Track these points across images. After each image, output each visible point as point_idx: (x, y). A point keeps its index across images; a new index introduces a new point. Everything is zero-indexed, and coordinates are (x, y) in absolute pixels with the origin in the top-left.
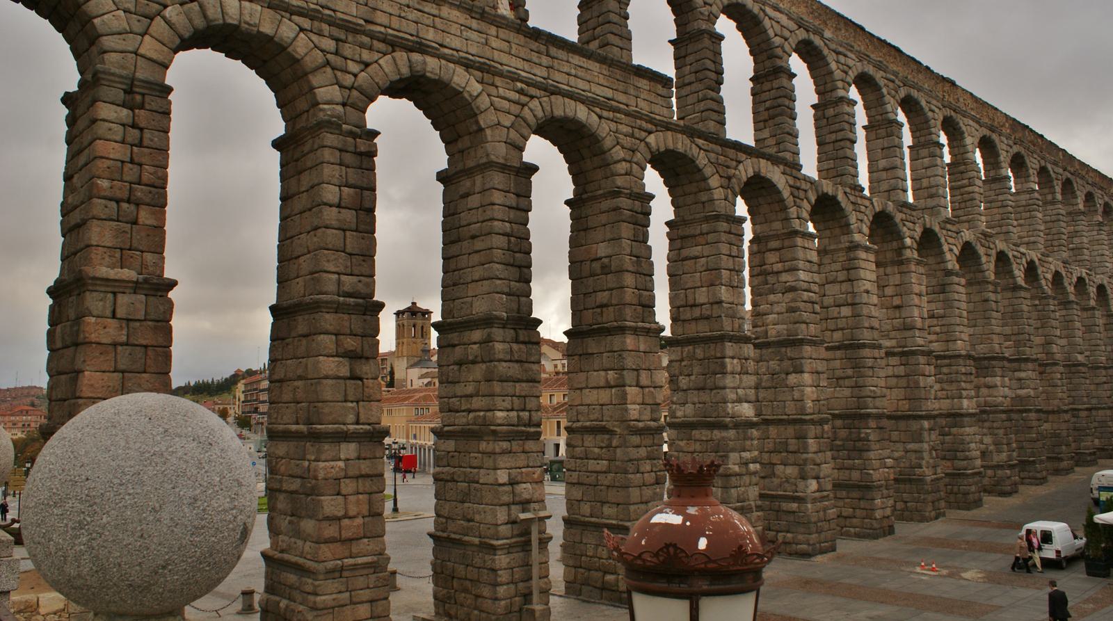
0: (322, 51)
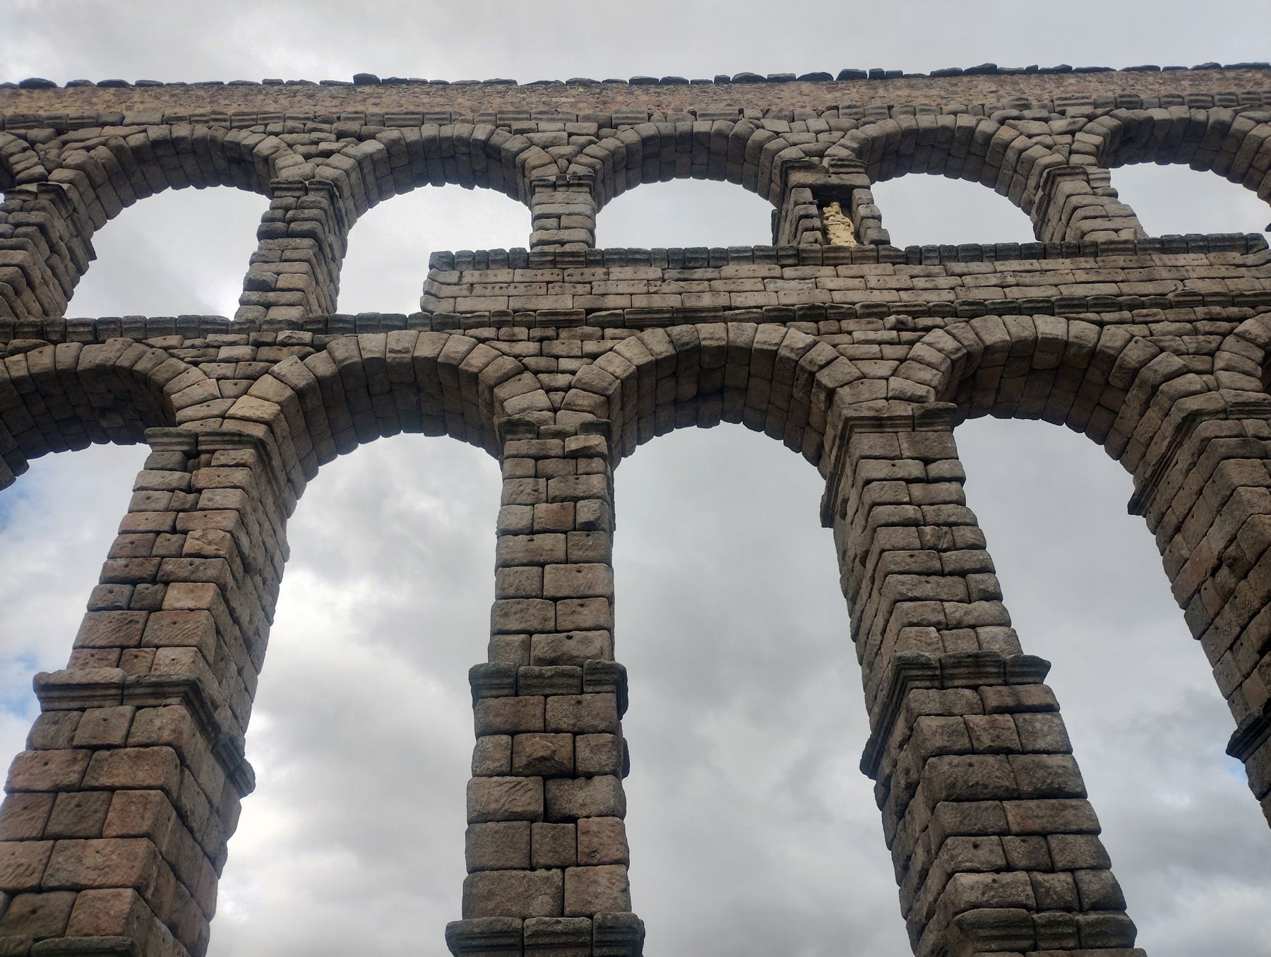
0: (516, 357)
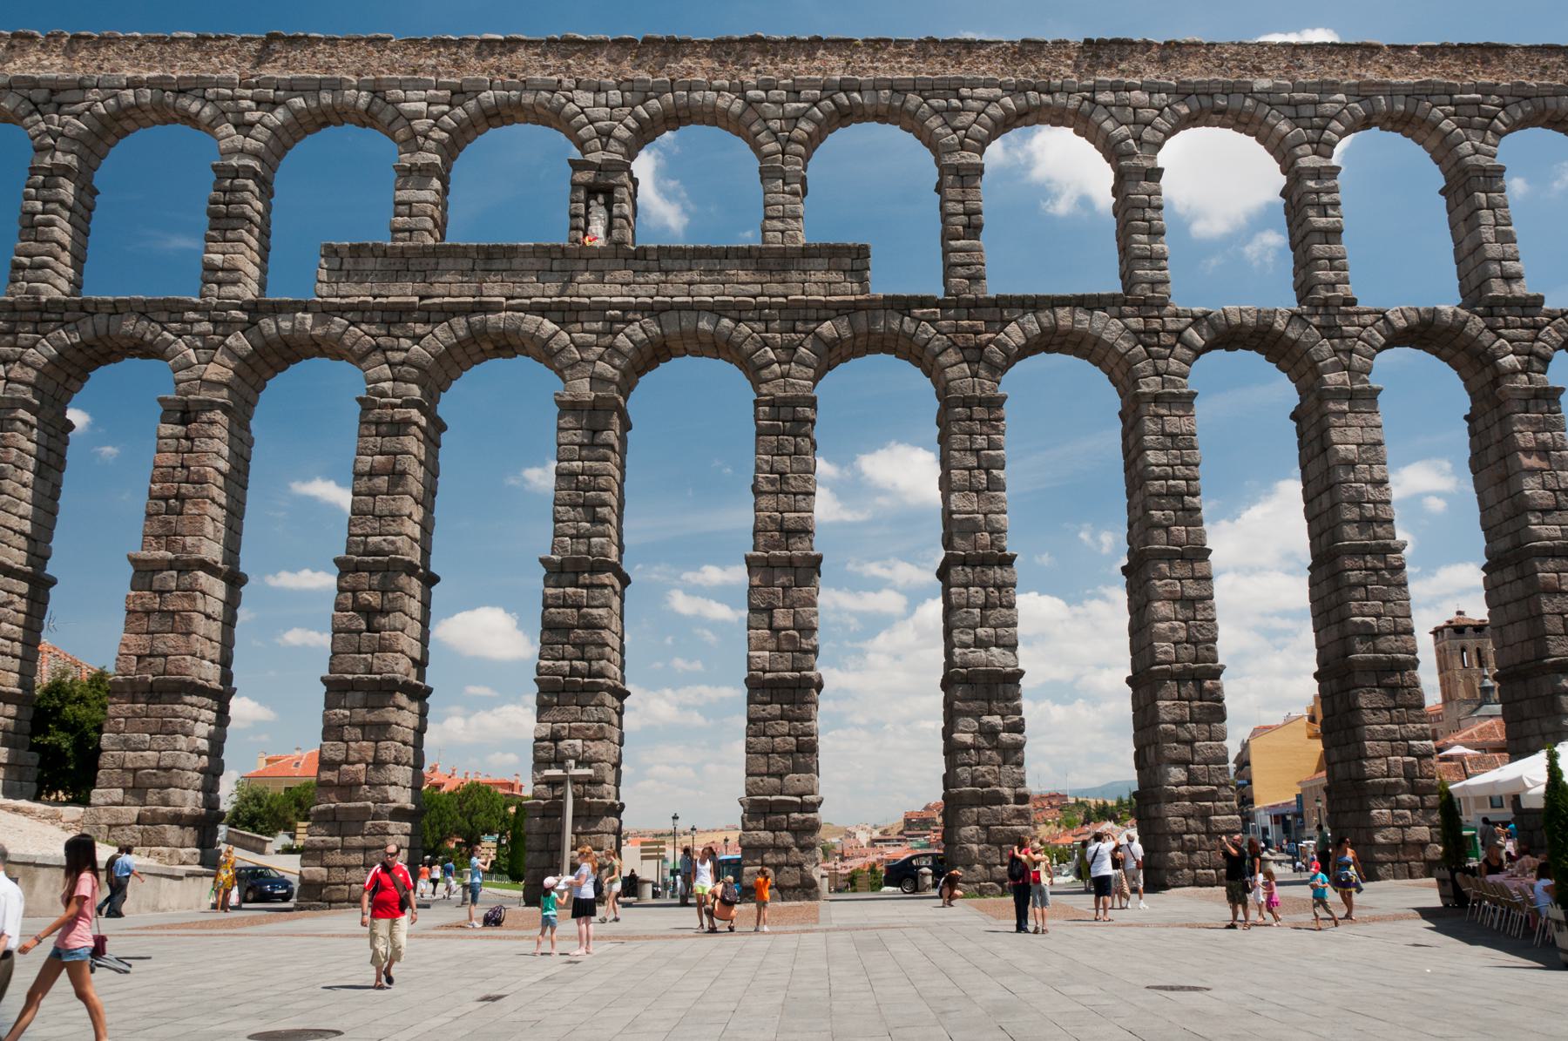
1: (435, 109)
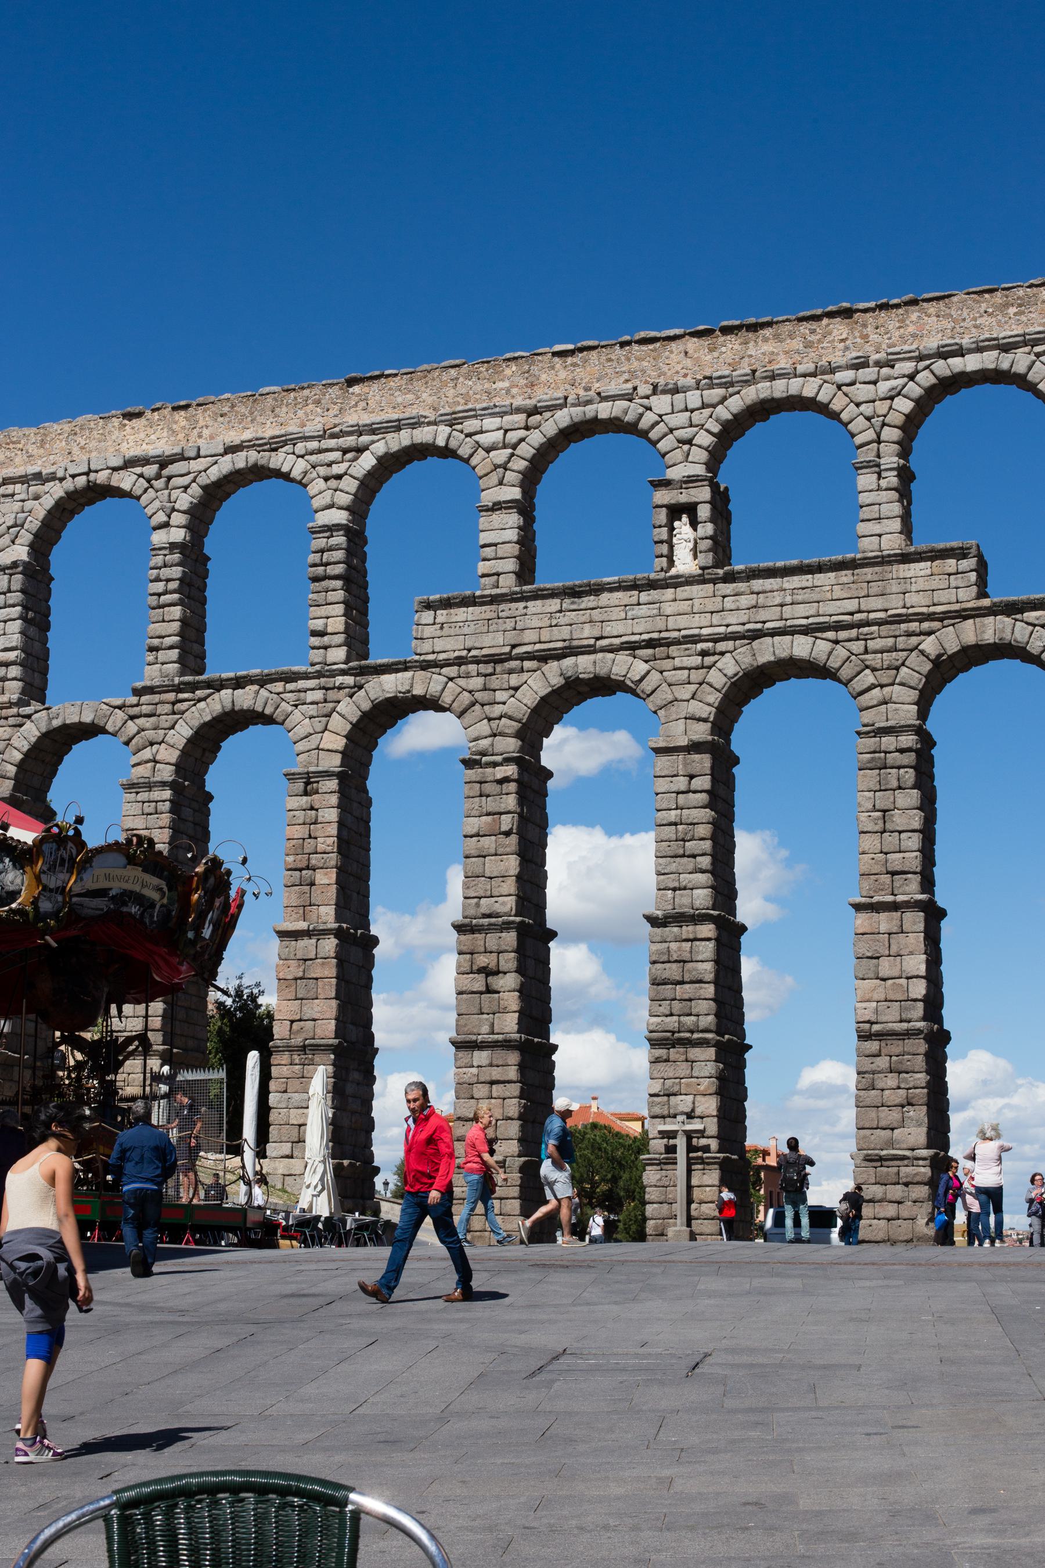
0: (470, 692)
1: (513, 437)
